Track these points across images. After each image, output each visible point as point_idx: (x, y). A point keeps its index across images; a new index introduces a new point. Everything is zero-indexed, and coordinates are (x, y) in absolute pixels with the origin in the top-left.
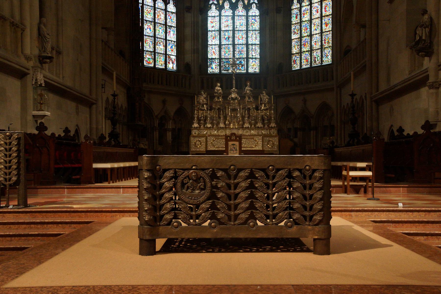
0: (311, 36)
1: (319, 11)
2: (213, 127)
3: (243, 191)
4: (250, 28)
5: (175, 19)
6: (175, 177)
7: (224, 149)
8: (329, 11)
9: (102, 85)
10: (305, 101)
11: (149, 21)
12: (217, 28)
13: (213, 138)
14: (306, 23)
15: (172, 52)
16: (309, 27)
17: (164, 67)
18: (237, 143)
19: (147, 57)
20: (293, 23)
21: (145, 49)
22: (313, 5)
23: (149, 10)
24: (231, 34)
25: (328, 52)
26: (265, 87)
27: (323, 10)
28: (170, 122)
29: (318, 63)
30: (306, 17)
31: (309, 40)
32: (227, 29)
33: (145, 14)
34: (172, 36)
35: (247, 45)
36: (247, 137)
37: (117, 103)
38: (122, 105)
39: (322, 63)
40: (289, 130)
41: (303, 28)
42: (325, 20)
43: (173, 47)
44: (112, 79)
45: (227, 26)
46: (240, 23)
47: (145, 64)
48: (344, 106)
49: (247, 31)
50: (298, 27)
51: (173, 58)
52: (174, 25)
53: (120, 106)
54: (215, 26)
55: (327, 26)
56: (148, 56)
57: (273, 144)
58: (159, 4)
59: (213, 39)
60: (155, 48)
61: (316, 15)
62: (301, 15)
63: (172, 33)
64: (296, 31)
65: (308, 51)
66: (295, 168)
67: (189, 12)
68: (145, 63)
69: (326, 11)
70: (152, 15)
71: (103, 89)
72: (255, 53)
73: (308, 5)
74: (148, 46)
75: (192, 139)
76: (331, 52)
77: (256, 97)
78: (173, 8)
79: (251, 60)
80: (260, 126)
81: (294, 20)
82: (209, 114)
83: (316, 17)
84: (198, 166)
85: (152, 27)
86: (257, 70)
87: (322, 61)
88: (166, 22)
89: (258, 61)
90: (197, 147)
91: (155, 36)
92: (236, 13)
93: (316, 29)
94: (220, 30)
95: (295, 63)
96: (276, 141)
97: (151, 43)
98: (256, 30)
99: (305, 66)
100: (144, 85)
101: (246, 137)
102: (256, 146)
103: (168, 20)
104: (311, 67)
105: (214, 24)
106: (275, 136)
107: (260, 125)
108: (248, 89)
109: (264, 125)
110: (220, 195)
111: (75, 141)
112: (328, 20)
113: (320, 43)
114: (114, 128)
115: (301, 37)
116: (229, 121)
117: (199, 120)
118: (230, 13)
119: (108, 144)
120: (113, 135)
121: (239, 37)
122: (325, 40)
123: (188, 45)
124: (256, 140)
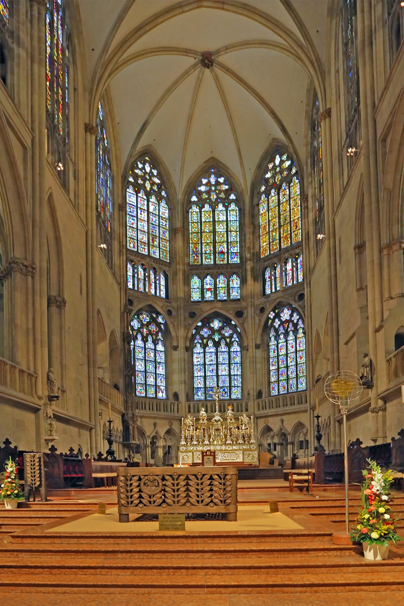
0: (287, 367)
1: (294, 346)
8: (303, 347)
10: (282, 421)
11: (140, 359)
12: (202, 362)
14: (283, 356)
15: (162, 384)
17: (154, 396)
19: (139, 388)
22: (288, 342)
24: (215, 367)
25: (303, 380)
27: (298, 346)
28: (161, 441)
29: (294, 389)
30: (283, 352)
32: (211, 363)
33: (137, 354)
34: (161, 370)
39: (297, 389)
44: (108, 408)
45: (211, 360)
46: (223, 358)
47: (137, 393)
50: (276, 360)
52: (163, 361)
53: (116, 429)
54: (200, 360)
57: (253, 456)
58: (149, 345)
60: (146, 381)
63: (161, 368)
64: (273, 363)
65: (285, 380)
67: (176, 350)
70: (143, 354)
73: (284, 342)
74: (140, 379)
75: (180, 454)
77: (237, 419)
78: (161, 347)
83: (292, 351)
87: (297, 387)
88: (155, 359)
89: (239, 389)
90: (184, 460)
91: (146, 371)
92: (219, 349)
93: (291, 362)
98: (237, 363)
100: (137, 411)
103: (158, 358)
105: (199, 359)
106: (255, 450)
107: (240, 441)
108: (230, 413)
109: (245, 442)
111: (78, 457)
113: (295, 373)
114: (110, 447)
115: (278, 368)
118: (213, 350)
119: (106, 460)
120: (110, 452)
121: (223, 369)
122: (300, 371)
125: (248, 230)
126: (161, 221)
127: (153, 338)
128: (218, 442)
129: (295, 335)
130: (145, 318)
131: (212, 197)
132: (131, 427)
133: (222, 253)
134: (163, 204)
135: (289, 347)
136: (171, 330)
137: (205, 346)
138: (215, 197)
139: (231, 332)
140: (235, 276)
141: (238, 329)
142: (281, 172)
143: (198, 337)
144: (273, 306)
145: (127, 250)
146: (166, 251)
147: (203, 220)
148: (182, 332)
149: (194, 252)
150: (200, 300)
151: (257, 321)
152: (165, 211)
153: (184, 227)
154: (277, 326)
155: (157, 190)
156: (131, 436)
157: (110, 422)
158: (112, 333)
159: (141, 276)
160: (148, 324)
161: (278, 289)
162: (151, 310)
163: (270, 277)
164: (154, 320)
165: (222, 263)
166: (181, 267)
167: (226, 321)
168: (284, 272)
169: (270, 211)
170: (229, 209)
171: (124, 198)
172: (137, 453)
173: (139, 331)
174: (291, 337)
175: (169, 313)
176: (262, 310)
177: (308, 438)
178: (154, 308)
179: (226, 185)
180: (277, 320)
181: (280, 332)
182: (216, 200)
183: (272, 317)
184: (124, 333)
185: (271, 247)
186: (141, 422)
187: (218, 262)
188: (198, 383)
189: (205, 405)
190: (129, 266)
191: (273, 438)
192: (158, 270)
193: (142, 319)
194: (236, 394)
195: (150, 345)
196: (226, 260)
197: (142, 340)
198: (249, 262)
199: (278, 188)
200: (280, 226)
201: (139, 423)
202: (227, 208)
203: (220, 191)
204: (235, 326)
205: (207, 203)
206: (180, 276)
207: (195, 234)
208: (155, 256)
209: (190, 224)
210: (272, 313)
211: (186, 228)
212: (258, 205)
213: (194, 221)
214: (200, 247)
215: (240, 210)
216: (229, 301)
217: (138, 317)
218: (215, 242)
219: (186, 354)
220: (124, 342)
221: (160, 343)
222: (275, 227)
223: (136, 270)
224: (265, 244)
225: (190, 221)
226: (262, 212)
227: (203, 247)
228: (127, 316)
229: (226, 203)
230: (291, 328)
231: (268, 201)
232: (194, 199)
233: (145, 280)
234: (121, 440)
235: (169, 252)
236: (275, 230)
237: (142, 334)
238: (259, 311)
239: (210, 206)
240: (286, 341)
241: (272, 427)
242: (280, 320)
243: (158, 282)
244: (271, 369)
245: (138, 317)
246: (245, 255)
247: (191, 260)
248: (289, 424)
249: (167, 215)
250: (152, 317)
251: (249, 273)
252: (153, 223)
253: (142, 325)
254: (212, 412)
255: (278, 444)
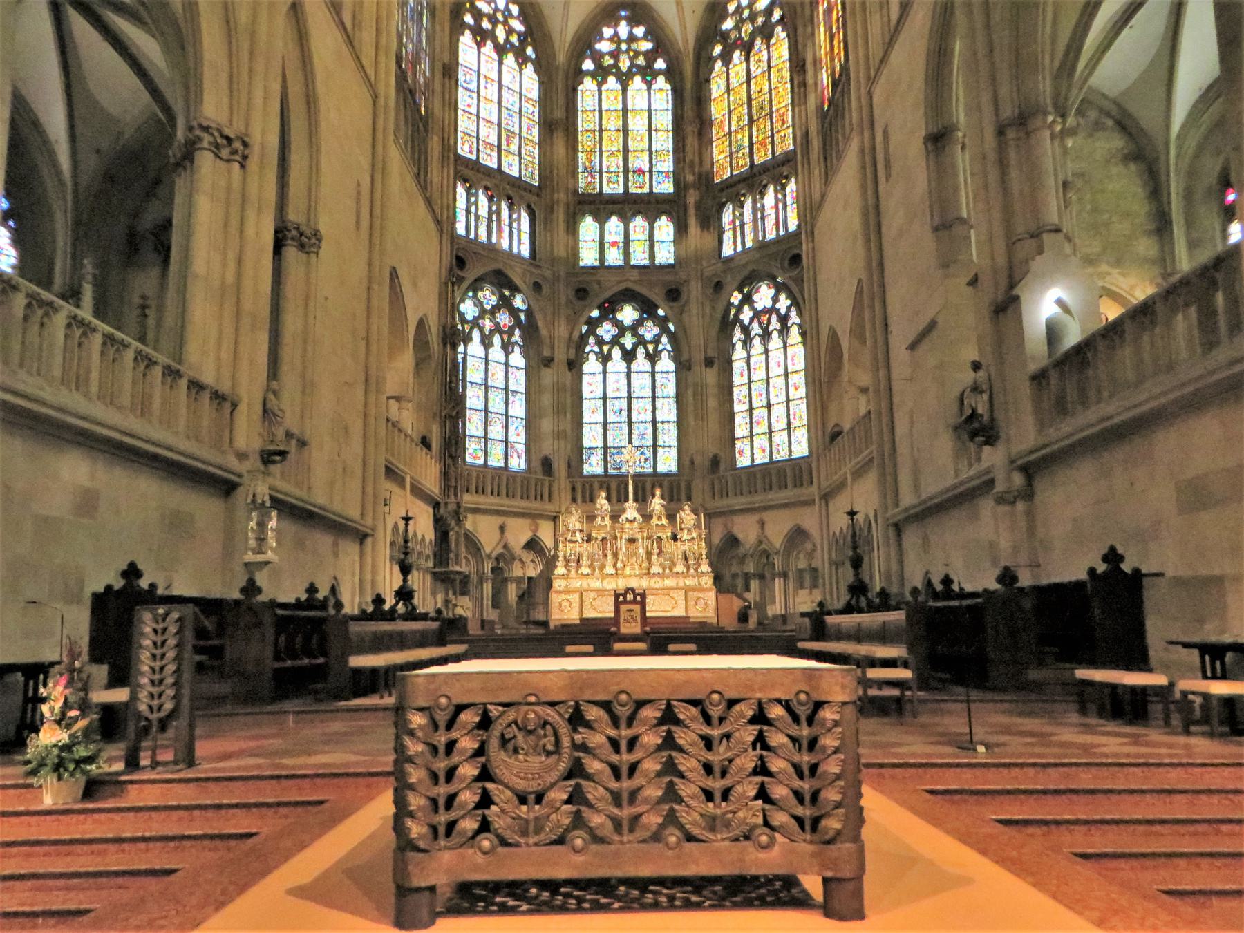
2: (593, 574)
3: (648, 756)
4: (659, 393)
5: (523, 378)
6: (485, 722)
7: (612, 615)
9: (385, 500)
10: (762, 524)
12: (599, 393)
13: (593, 595)
14: (759, 383)
15: (518, 437)
16: (764, 392)
17: (502, 465)
18: (637, 608)
20: (736, 383)
21: (467, 433)
23: (476, 364)
26: (689, 499)
29: (782, 455)
31: (766, 414)
34: (518, 408)
35: (654, 422)
36: (656, 592)
37: (415, 531)
38: (423, 536)
40: (735, 576)
41: (754, 394)
42: (793, 379)
43: (520, 428)
46: (641, 384)
48: (834, 533)
49: (654, 398)
50: (745, 389)
51: (521, 448)
53: (420, 538)
55: (796, 389)
56: (474, 446)
57: (706, 604)
59: (593, 412)
61: (776, 370)
62: (749, 370)
63: (518, 403)
64: (741, 398)
66: (774, 697)
68: (468, 459)
69: (793, 364)
71: (387, 507)
72: (669, 435)
76: (806, 435)
77: (671, 517)
79: (660, 450)
80: (680, 571)
81: (737, 379)
82: (585, 549)
84: (540, 695)
85: (482, 394)
86: (674, 469)
87: (790, 451)
89: (674, 452)
91: (486, 411)
92: (634, 366)
94: (604, 398)
95: (741, 455)
96: (710, 597)
97: (479, 422)
99: (761, 459)
101: (654, 591)
102: (673, 608)
104: (771, 462)
106: (710, 590)
107: (680, 568)
108: (657, 504)
109: (688, 568)
110: (593, 766)
112: (799, 380)
114: (405, 580)
115: (751, 410)
116: (622, 562)
117: (567, 561)
118: (622, 366)
123: (547, 425)
124: (673, 598)
125: (691, 129)
126: (524, 103)
127: (502, 340)
128: (633, 569)
129: (783, 340)
130: (489, 297)
131: (621, 64)
132: (451, 533)
133: (640, 171)
134: (529, 69)
135: (772, 364)
136: (540, 324)
137: (605, 359)
138: (628, 63)
139: (656, 330)
140: (664, 218)
141: (672, 327)
142: (752, 17)
143: (592, 340)
144: (739, 278)
145: (458, 158)
146: (532, 163)
147: (604, 107)
148: (562, 328)
149: (586, 169)
150: (597, 264)
151: (708, 311)
152: (532, 86)
153: (567, 118)
154: (746, 322)
155: (517, 44)
156: (451, 555)
157: (407, 519)
158: (421, 324)
159: (483, 211)
160: (495, 310)
161: (749, 244)
162: (501, 280)
163: (733, 222)
164: (505, 303)
165: (639, 191)
166: (562, 196)
167: (647, 309)
168: (758, 211)
169: (731, 93)
170: (654, 87)
171: (454, 52)
172: (463, 593)
173: (475, 323)
174: (775, 342)
175: (537, 287)
176: (718, 286)
177: (817, 563)
178: (506, 276)
179: (648, 41)
180: (746, 308)
181: (752, 334)
182: (630, 68)
183: (736, 303)
184: (444, 328)
185: (734, 162)
186: (474, 523)
187: (632, 190)
188: (591, 437)
189: (605, 486)
190: (461, 191)
191: (742, 560)
192: (515, 200)
193: (482, 299)
194: (668, 462)
195: (496, 353)
196: (647, 186)
197: (482, 342)
198: (691, 191)
199: (748, 48)
200: (751, 121)
201: (468, 525)
202: (649, 85)
203: (637, 54)
204: (665, 320)
205: (614, 75)
206: (560, 215)
207: (589, 133)
208: (510, 173)
209: (580, 113)
210: (736, 293)
211: (570, 120)
212: (708, 81)
213: (588, 108)
214: (598, 158)
215: (674, 90)
216: (652, 269)
217: (475, 296)
218: (626, 150)
219: (569, 374)
220: (445, 345)
221: (517, 349)
222: (741, 123)
223: (473, 199)
224: (722, 156)
225: (580, 108)
226: (714, 94)
227: (604, 158)
228: (453, 291)
229: (648, 73)
230: (775, 324)
231: (728, 74)
232: (588, 65)
233: (490, 219)
234: (431, 564)
235: (539, 165)
236: (742, 128)
237: (482, 330)
238: (711, 290)
239: (619, 79)
240: (766, 352)
241: (740, 536)
242: (753, 308)
243: (515, 225)
244: (736, 410)
245: (475, 296)
246: (685, 177)
247: (582, 184)
248: (777, 529)
249: (535, 94)
250: (502, 297)
251: (692, 211)
252: (510, 107)
253: (483, 312)
254: (619, 501)
255: (754, 575)
